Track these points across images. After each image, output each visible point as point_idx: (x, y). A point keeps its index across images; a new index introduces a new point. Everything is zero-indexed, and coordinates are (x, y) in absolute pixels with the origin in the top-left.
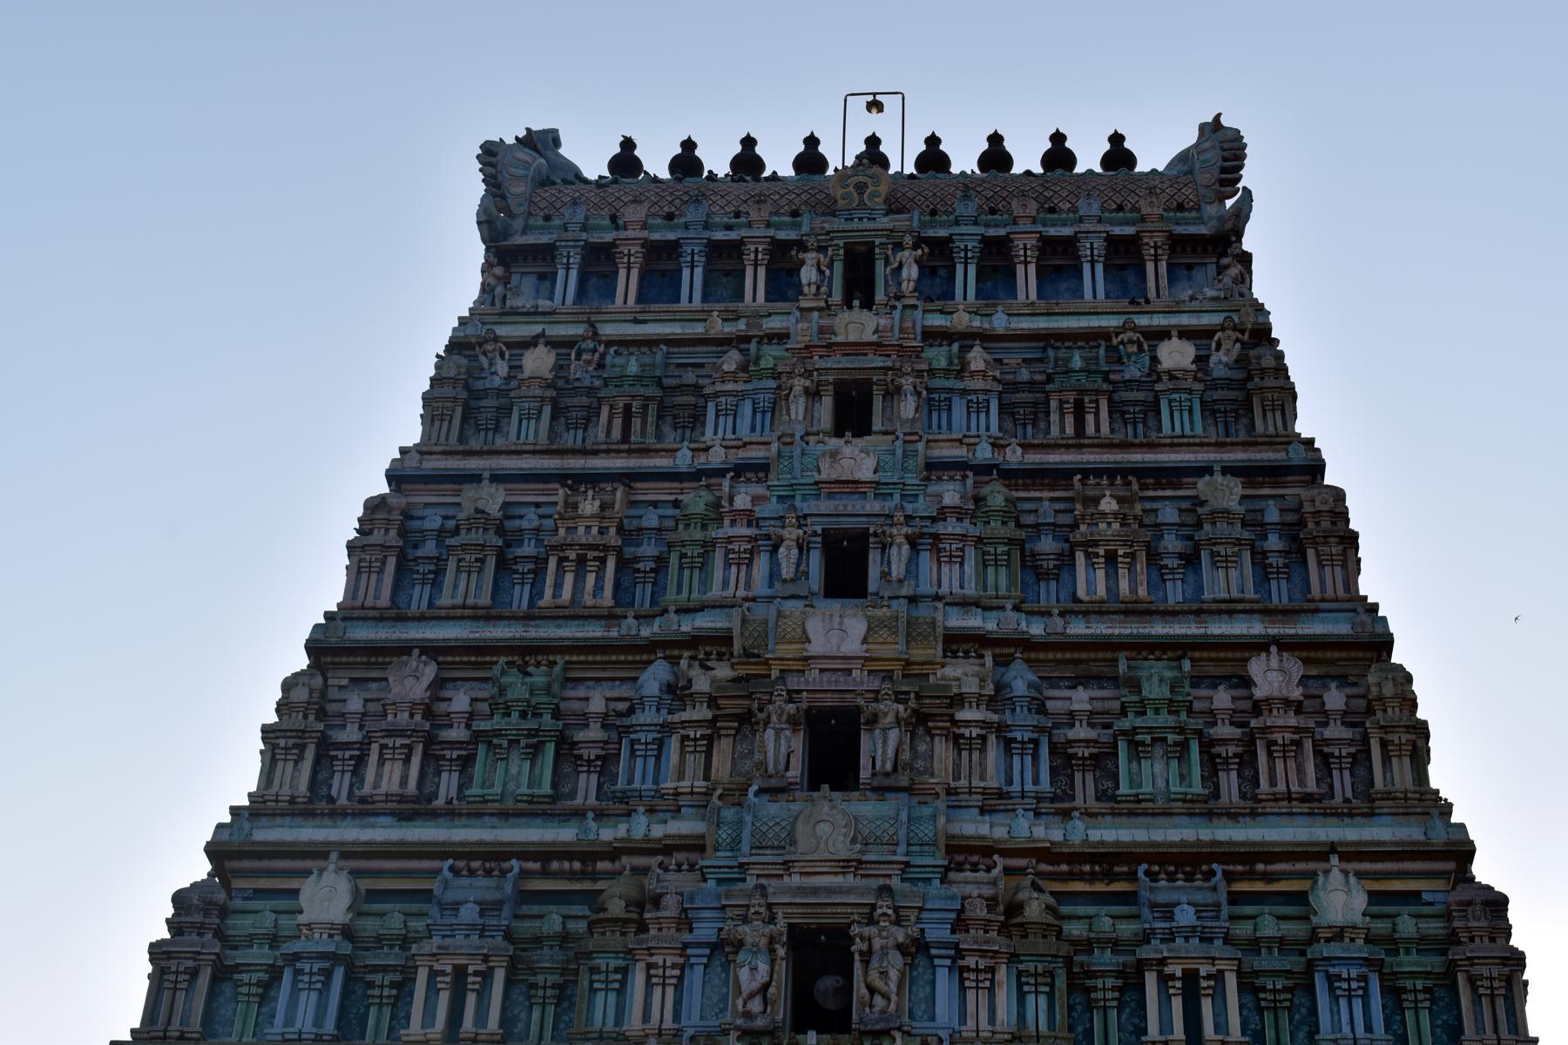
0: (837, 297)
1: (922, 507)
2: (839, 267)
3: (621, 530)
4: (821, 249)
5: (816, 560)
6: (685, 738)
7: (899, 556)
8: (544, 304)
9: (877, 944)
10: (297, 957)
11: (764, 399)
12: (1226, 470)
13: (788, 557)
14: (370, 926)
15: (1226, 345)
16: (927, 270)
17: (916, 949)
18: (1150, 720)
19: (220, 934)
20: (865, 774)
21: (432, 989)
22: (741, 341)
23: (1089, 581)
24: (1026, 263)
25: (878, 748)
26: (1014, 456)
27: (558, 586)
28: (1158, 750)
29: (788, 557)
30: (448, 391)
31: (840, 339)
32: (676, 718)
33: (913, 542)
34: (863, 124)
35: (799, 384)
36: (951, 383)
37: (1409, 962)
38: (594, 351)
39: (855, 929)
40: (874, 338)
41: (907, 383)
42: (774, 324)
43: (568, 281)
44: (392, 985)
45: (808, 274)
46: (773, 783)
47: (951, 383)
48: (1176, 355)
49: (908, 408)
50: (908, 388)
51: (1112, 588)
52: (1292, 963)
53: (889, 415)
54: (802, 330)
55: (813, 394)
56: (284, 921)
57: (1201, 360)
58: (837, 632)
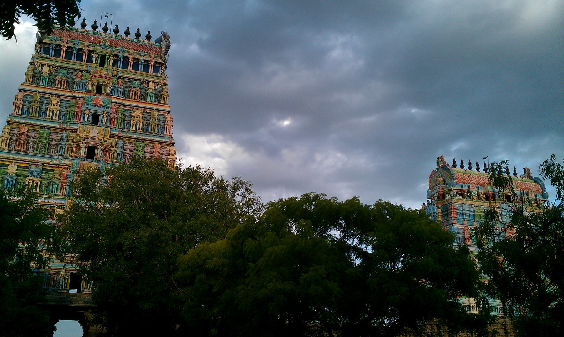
1: (109, 111)
3: (60, 106)
4: (97, 54)
20: (96, 157)
25: (98, 153)
30: (30, 73)
32: (67, 143)
33: (107, 117)
34: (105, 20)
45: (94, 60)
53: (105, 90)
55: (93, 84)
58: (94, 132)
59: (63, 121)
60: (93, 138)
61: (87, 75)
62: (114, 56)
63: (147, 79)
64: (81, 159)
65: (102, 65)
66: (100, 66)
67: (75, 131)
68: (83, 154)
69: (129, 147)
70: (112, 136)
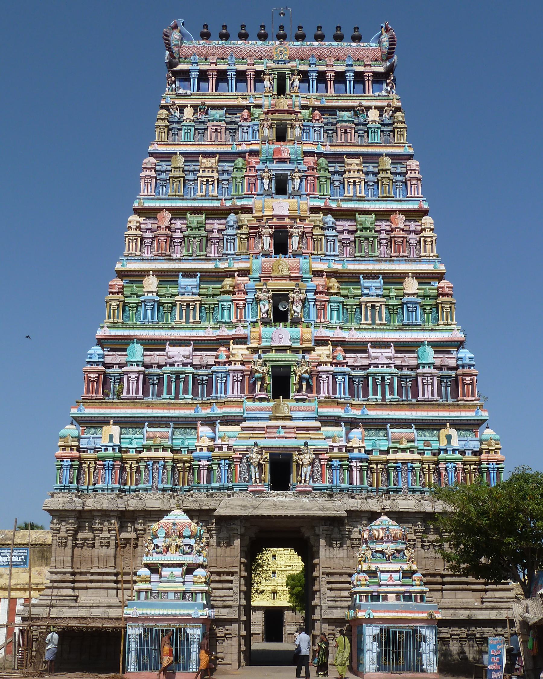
0: (275, 92)
2: (275, 80)
5: (273, 182)
6: (241, 238)
7: (297, 181)
8: (188, 92)
9: (296, 299)
10: (145, 301)
11: (256, 128)
12: (387, 155)
13: (266, 182)
14: (162, 291)
15: (388, 111)
16: (301, 81)
17: (304, 301)
18: (364, 233)
19: (123, 294)
20: (289, 250)
21: (181, 310)
22: (248, 107)
23: (349, 191)
24: (330, 81)
25: (294, 243)
26: (328, 149)
27: (201, 189)
28: (366, 242)
29: (266, 182)
31: (277, 108)
33: (300, 178)
35: (266, 124)
36: (310, 124)
37: (427, 301)
38: (204, 109)
39: (290, 295)
40: (287, 108)
41: (297, 124)
42: (259, 102)
43: (194, 82)
44: (170, 307)
46: (266, 253)
47: (310, 124)
48: (373, 115)
49: (297, 132)
50: (297, 125)
51: (355, 192)
52: (399, 302)
54: (266, 102)
55: (270, 127)
56: (139, 289)
57: (381, 115)
58: (282, 206)
59: (227, 197)
60: (281, 217)
61: (259, 111)
62: (300, 72)
63: (365, 103)
64: (266, 255)
65: (281, 90)
66: (279, 94)
67: (248, 210)
68: (266, 247)
69: (347, 225)
70: (314, 210)
